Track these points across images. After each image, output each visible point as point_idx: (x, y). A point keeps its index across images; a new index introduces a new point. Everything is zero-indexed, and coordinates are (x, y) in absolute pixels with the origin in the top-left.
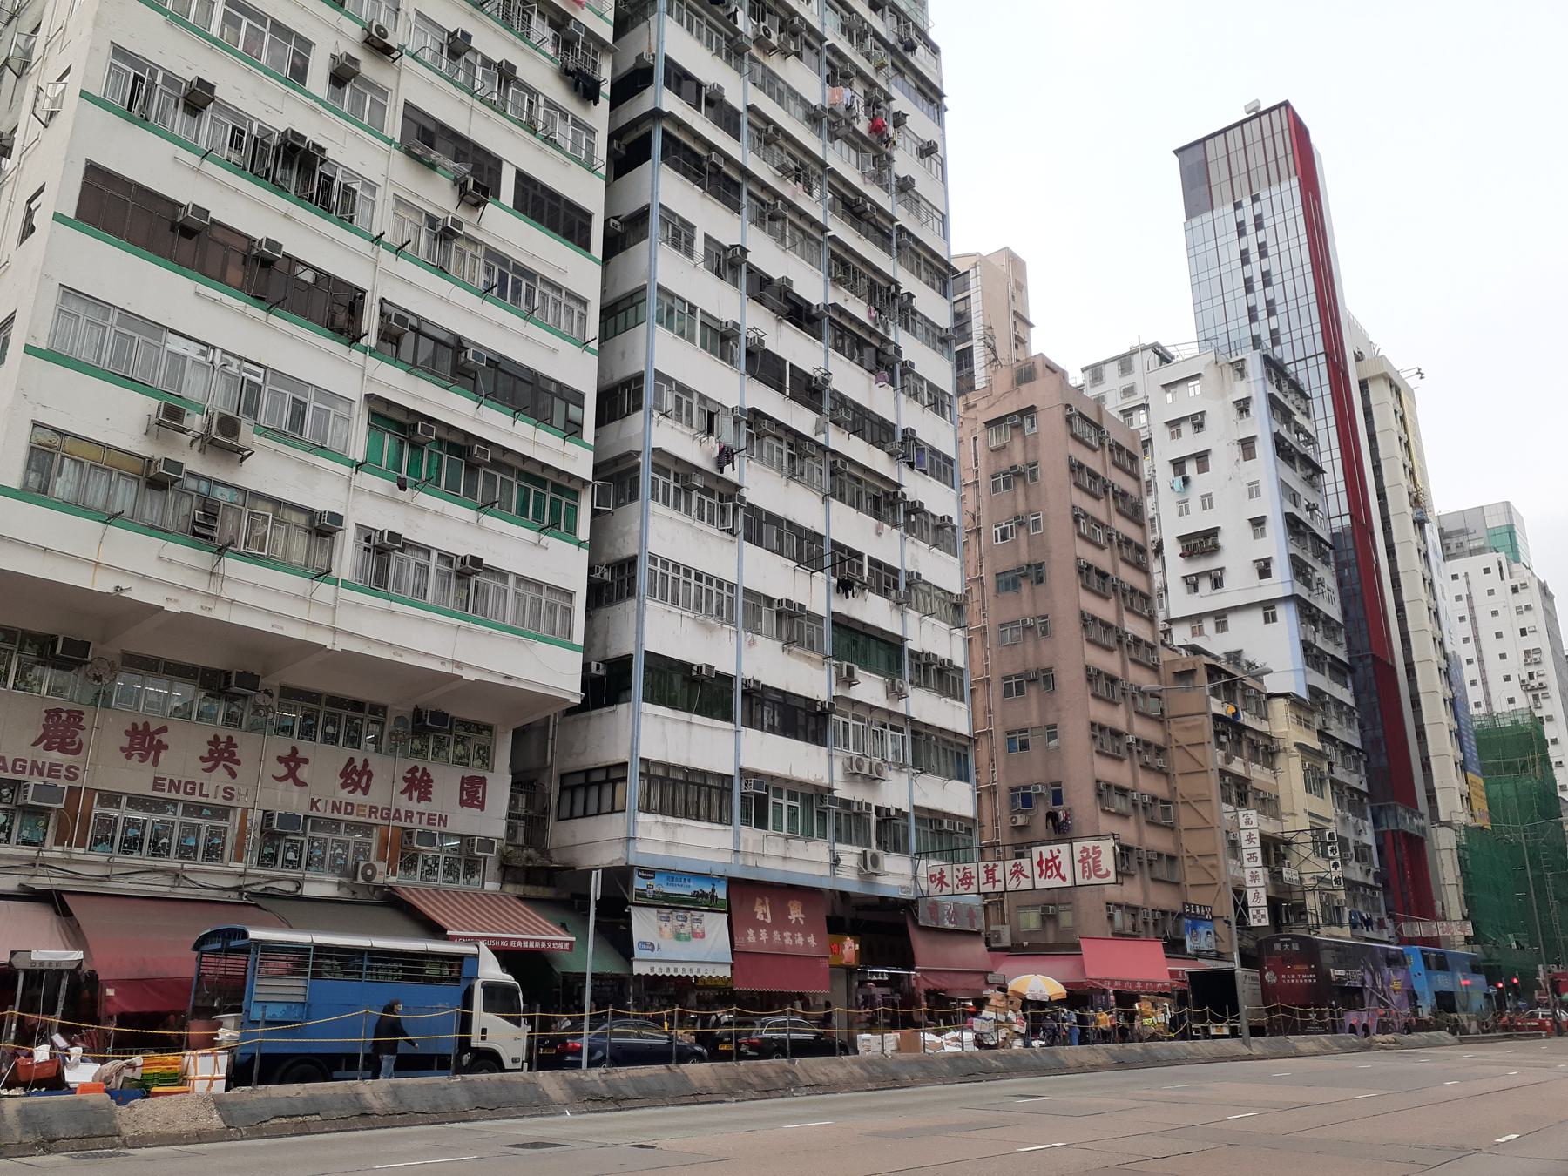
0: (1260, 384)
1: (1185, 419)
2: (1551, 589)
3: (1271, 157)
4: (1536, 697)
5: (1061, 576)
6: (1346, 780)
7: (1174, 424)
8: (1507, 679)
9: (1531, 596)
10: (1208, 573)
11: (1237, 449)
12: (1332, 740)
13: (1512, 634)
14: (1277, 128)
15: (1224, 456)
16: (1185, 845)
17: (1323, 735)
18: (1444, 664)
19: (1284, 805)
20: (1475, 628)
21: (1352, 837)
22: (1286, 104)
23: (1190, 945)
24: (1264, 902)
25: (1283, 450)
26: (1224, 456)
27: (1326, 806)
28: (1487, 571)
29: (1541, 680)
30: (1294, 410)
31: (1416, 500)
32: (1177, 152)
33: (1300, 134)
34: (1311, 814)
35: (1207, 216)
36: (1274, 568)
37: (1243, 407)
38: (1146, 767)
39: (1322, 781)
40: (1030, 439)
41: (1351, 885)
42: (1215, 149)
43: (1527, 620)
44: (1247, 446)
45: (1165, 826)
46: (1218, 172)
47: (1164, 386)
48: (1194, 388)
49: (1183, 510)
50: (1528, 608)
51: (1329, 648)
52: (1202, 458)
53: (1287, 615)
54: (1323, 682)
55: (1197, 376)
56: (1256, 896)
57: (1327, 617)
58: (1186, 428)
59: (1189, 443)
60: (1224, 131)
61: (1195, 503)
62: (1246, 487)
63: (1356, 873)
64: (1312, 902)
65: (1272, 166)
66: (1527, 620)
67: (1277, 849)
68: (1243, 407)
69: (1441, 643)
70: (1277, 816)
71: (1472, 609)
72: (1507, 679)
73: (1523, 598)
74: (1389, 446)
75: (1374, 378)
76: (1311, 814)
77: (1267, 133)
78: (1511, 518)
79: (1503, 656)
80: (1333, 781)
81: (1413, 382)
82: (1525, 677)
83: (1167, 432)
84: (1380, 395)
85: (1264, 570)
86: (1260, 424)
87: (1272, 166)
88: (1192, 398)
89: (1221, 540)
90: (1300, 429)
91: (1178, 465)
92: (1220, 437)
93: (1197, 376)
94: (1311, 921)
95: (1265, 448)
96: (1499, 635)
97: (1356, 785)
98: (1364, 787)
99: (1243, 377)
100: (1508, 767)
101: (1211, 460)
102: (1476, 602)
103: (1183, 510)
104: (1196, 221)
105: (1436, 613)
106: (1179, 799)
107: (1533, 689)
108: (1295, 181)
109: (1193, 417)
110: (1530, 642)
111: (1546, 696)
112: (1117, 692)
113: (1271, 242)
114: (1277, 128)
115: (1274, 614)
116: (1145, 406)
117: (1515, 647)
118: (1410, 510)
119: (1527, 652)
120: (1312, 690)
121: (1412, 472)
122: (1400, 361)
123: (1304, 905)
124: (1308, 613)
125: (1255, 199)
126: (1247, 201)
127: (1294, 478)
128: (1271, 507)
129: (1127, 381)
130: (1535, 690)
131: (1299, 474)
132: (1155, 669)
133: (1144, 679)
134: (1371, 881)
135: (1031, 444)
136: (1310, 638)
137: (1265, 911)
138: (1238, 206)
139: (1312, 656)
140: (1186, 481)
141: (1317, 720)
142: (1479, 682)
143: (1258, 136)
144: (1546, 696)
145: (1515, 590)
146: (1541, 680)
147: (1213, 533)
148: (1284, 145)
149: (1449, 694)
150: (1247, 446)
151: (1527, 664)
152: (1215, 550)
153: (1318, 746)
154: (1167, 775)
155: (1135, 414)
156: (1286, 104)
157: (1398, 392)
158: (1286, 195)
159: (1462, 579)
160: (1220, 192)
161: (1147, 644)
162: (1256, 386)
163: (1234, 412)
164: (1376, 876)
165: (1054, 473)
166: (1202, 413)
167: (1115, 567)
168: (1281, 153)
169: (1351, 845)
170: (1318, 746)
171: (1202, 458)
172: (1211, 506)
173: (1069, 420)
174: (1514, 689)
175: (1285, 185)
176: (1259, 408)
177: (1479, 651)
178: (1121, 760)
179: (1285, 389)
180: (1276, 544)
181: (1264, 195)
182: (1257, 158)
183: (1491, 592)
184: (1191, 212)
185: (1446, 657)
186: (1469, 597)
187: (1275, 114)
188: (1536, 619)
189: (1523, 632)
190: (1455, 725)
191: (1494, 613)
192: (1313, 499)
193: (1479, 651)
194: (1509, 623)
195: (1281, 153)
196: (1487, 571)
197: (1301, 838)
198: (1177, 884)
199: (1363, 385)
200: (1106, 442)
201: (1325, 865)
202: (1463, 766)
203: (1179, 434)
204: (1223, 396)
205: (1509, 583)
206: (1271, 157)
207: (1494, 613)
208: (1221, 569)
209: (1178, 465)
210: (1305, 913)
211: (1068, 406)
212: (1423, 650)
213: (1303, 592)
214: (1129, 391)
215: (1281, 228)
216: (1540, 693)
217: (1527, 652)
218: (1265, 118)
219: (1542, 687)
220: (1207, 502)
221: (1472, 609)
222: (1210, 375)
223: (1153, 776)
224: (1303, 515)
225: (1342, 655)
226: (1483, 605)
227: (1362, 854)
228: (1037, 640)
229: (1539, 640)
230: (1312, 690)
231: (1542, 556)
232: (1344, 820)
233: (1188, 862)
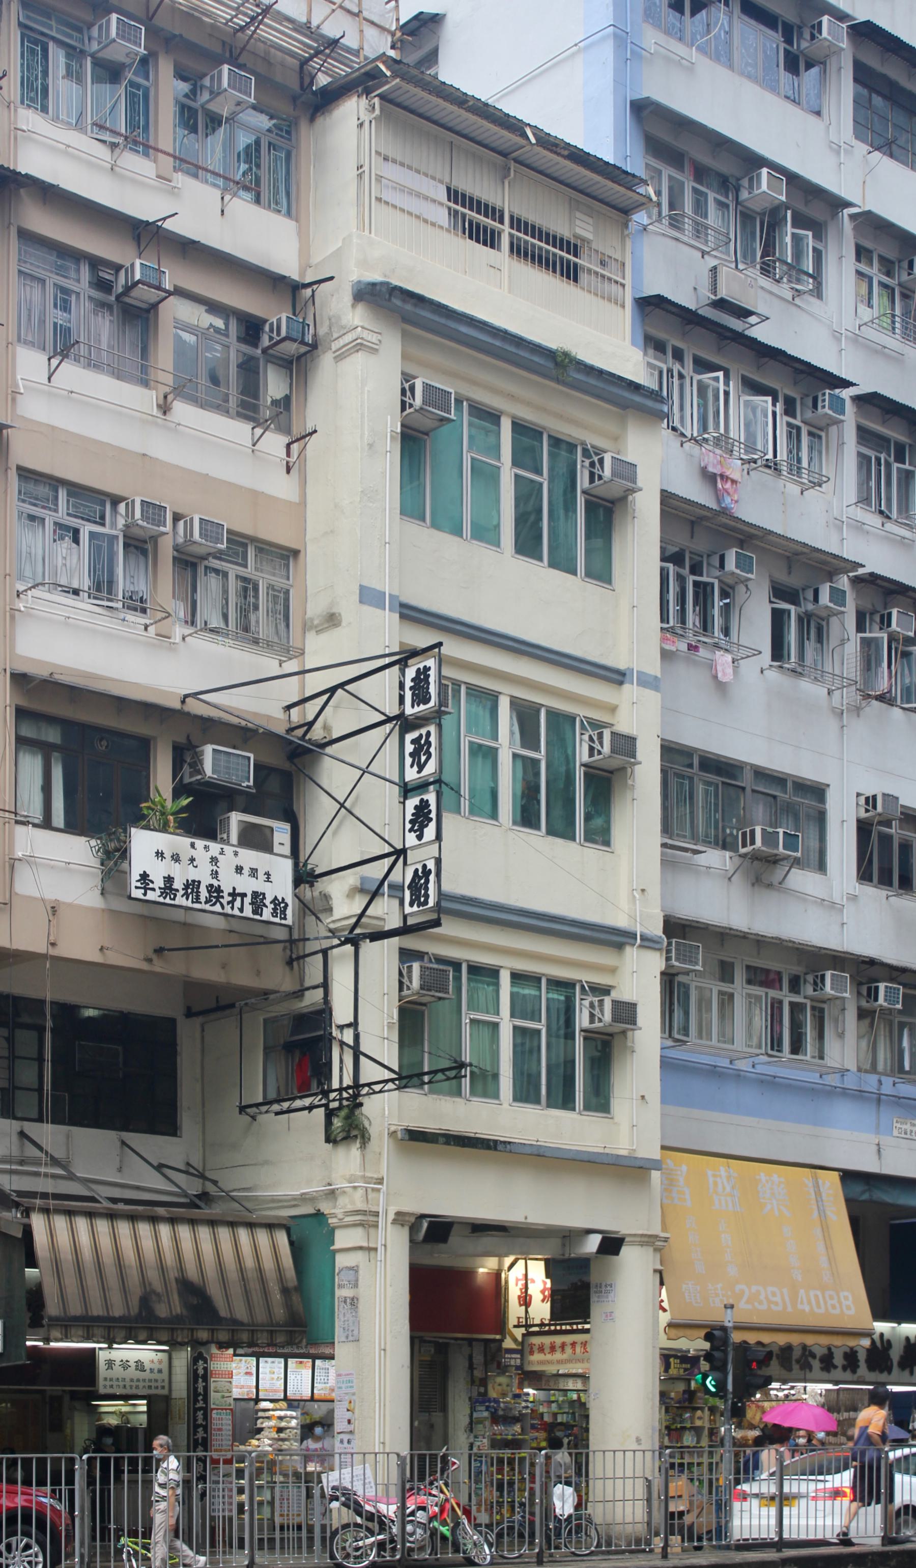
34: (410, 614)
64: (364, 997)
67: (185, 755)
94: (341, 1073)
120: (644, 112)
123: (324, 1012)
170: (630, 361)
197: (340, 718)
230: (662, 130)
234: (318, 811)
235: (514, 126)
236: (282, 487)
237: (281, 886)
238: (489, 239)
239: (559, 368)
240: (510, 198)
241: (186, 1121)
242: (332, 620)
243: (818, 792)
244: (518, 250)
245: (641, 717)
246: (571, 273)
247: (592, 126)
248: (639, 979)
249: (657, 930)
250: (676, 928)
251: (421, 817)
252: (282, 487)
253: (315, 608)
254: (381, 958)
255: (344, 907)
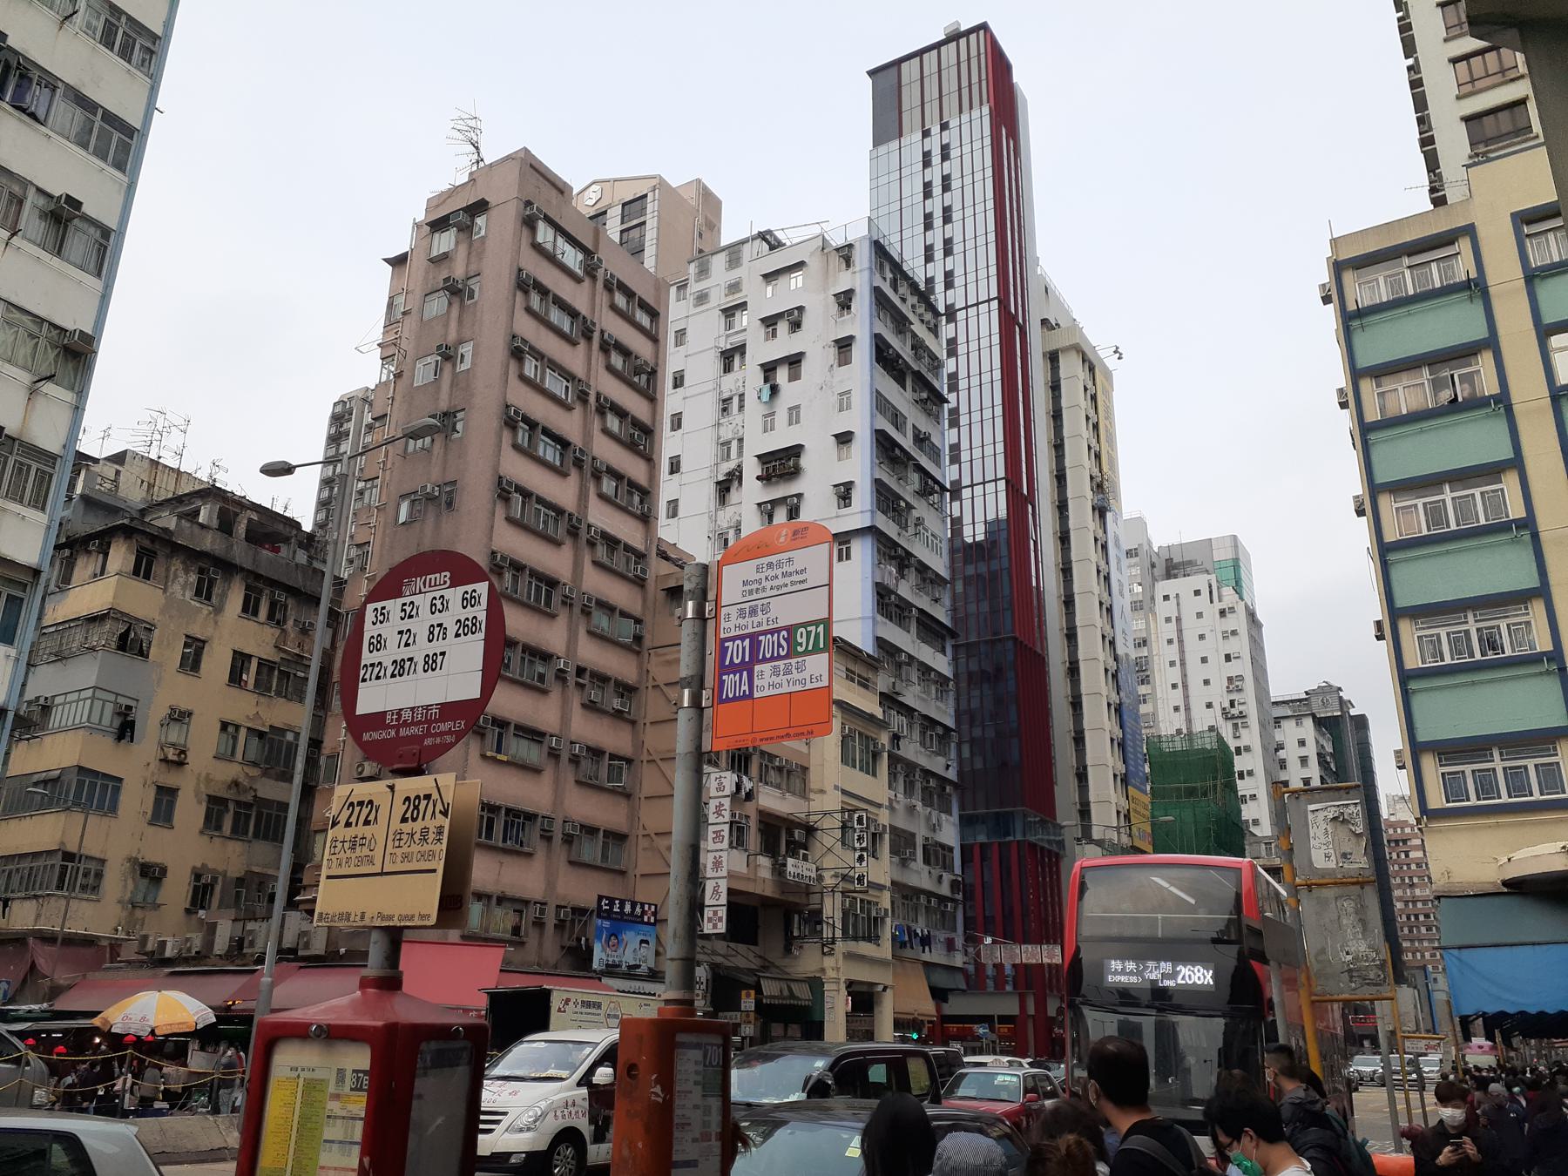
0: (866, 274)
1: (780, 316)
2: (1260, 616)
3: (965, 83)
4: (1236, 726)
5: (480, 424)
6: (924, 761)
7: (770, 322)
8: (1209, 706)
9: (1238, 621)
10: (782, 501)
11: (833, 351)
12: (908, 711)
13: (1216, 659)
14: (974, 52)
15: (818, 359)
16: (644, 820)
17: (889, 700)
18: (1112, 665)
19: (814, 780)
20: (1182, 652)
21: (921, 833)
22: (984, 27)
23: (599, 956)
24: (723, 900)
25: (884, 356)
26: (818, 359)
27: (876, 787)
28: (1197, 593)
29: (1241, 708)
30: (911, 316)
31: (1100, 486)
32: (871, 73)
33: (1000, 67)
34: (844, 792)
35: (894, 144)
36: (856, 495)
37: (845, 301)
38: (590, 706)
39: (876, 756)
40: (475, 245)
41: (905, 893)
42: (910, 70)
43: (1233, 646)
44: (844, 345)
45: (612, 791)
46: (910, 97)
47: (765, 276)
48: (796, 280)
49: (768, 427)
50: (1234, 633)
51: (923, 602)
52: (794, 361)
53: (862, 551)
54: (905, 639)
55: (800, 265)
56: (716, 891)
57: (920, 562)
58: (783, 327)
59: (785, 344)
60: (920, 53)
61: (781, 416)
62: (836, 397)
63: (921, 876)
64: (832, 908)
65: (965, 92)
66: (1233, 646)
67: (790, 833)
68: (845, 301)
69: (1112, 643)
70: (804, 794)
71: (1180, 631)
72: (1209, 706)
73: (1231, 622)
74: (1075, 425)
75: (1066, 349)
76: (844, 792)
77: (963, 57)
78: (1237, 553)
79: (1206, 682)
80: (894, 760)
81: (1111, 362)
82: (1227, 705)
83: (762, 331)
84: (1070, 367)
85: (844, 493)
86: (861, 324)
87: (965, 92)
88: (794, 289)
89: (804, 462)
90: (918, 346)
91: (769, 369)
92: (814, 341)
93: (800, 265)
94: (827, 933)
95: (862, 352)
96: (1204, 660)
97: (941, 772)
98: (952, 774)
99: (848, 265)
100: (1191, 792)
101: (805, 365)
102: (1185, 625)
103: (768, 427)
104: (883, 149)
105: (1110, 610)
106: (645, 757)
107: (1233, 717)
108: (986, 110)
109: (790, 312)
110: (1234, 669)
111: (1246, 726)
112: (556, 599)
113: (956, 175)
114: (974, 52)
115: (848, 549)
116: (743, 306)
117: (1219, 673)
118: (1089, 494)
119: (1230, 679)
120: (880, 642)
121: (1098, 456)
122: (1098, 337)
123: (820, 912)
124: (891, 552)
125: (944, 127)
126: (935, 129)
127: (903, 399)
128: (860, 420)
129: (733, 275)
130: (1235, 717)
131: (909, 394)
132: (640, 582)
133: (619, 593)
134: (945, 890)
135: (476, 250)
136: (890, 582)
137: (723, 912)
138: (926, 134)
139: (887, 602)
140: (774, 390)
141: (883, 682)
142: (1182, 708)
143: (954, 61)
144: (1246, 726)
145: (1222, 613)
146: (1241, 708)
147: (795, 451)
148: (979, 72)
149: (1115, 698)
150: (844, 345)
151: (1229, 691)
152: (795, 473)
153: (878, 712)
154: (633, 723)
155: (738, 314)
156: (984, 27)
157: (1092, 369)
158: (976, 124)
159: (1173, 600)
160: (911, 118)
161: (628, 548)
162: (860, 278)
163: (835, 308)
164: (954, 885)
165: (493, 289)
166: (801, 309)
167: (587, 435)
168: (975, 79)
169: (919, 842)
170: (878, 712)
171: (794, 361)
172: (797, 422)
173: (529, 223)
174: (1214, 718)
175: (976, 114)
176: (862, 303)
177: (1184, 676)
178: (544, 692)
179: (901, 290)
180: (860, 465)
181: (953, 123)
182: (950, 85)
183: (1199, 615)
184: (877, 142)
185: (1116, 659)
186: (1179, 620)
187: (973, 37)
188: (1241, 645)
189: (1228, 658)
190: (1118, 733)
191: (1202, 637)
192: (925, 425)
193: (1184, 676)
194: (1215, 648)
195: (975, 79)
196: (1197, 593)
197: (827, 823)
198: (622, 873)
199: (1053, 358)
200: (600, 274)
201: (850, 858)
202: (1125, 780)
203: (774, 335)
204: (825, 290)
205: (1218, 606)
206: (965, 83)
207: (1202, 637)
208: (799, 496)
209: (769, 369)
210: (820, 922)
211: (528, 203)
212: (1091, 649)
213: (891, 529)
214: (734, 287)
215: (967, 158)
216: (1239, 721)
217: (1230, 679)
218: (963, 41)
219: (1242, 716)
220: (794, 413)
221: (1180, 631)
222: (814, 264)
223: (606, 721)
224: (906, 442)
225: (941, 614)
226: (1191, 628)
227: (935, 854)
228: (439, 515)
229: (1243, 667)
230: (880, 642)
231: (1264, 590)
232: (911, 809)
233: (643, 843)
234: (817, 850)
235: (860, 651)
236: (804, 749)
237: (814, 875)
238: (852, 680)
239: (871, 718)
240: (857, 669)
241: (760, 941)
242: (822, 791)
243: (913, 835)
244: (860, 683)
245: (884, 818)
246: (866, 687)
247: (868, 647)
248: (885, 900)
249: (888, 884)
250: (893, 883)
251: (861, 859)
252: (804, 749)
253: (813, 786)
254: (838, 896)
255: (829, 880)
